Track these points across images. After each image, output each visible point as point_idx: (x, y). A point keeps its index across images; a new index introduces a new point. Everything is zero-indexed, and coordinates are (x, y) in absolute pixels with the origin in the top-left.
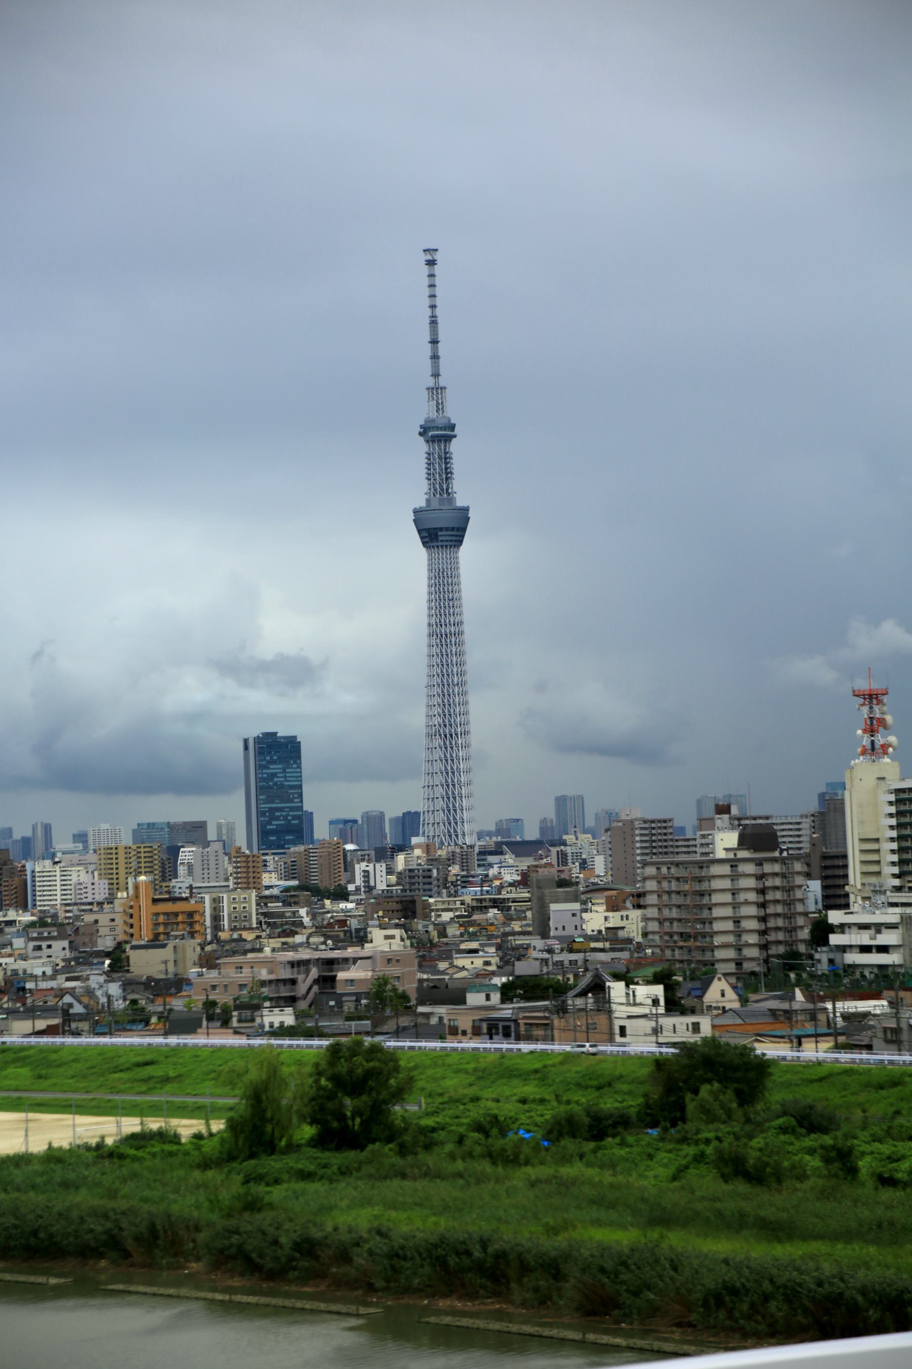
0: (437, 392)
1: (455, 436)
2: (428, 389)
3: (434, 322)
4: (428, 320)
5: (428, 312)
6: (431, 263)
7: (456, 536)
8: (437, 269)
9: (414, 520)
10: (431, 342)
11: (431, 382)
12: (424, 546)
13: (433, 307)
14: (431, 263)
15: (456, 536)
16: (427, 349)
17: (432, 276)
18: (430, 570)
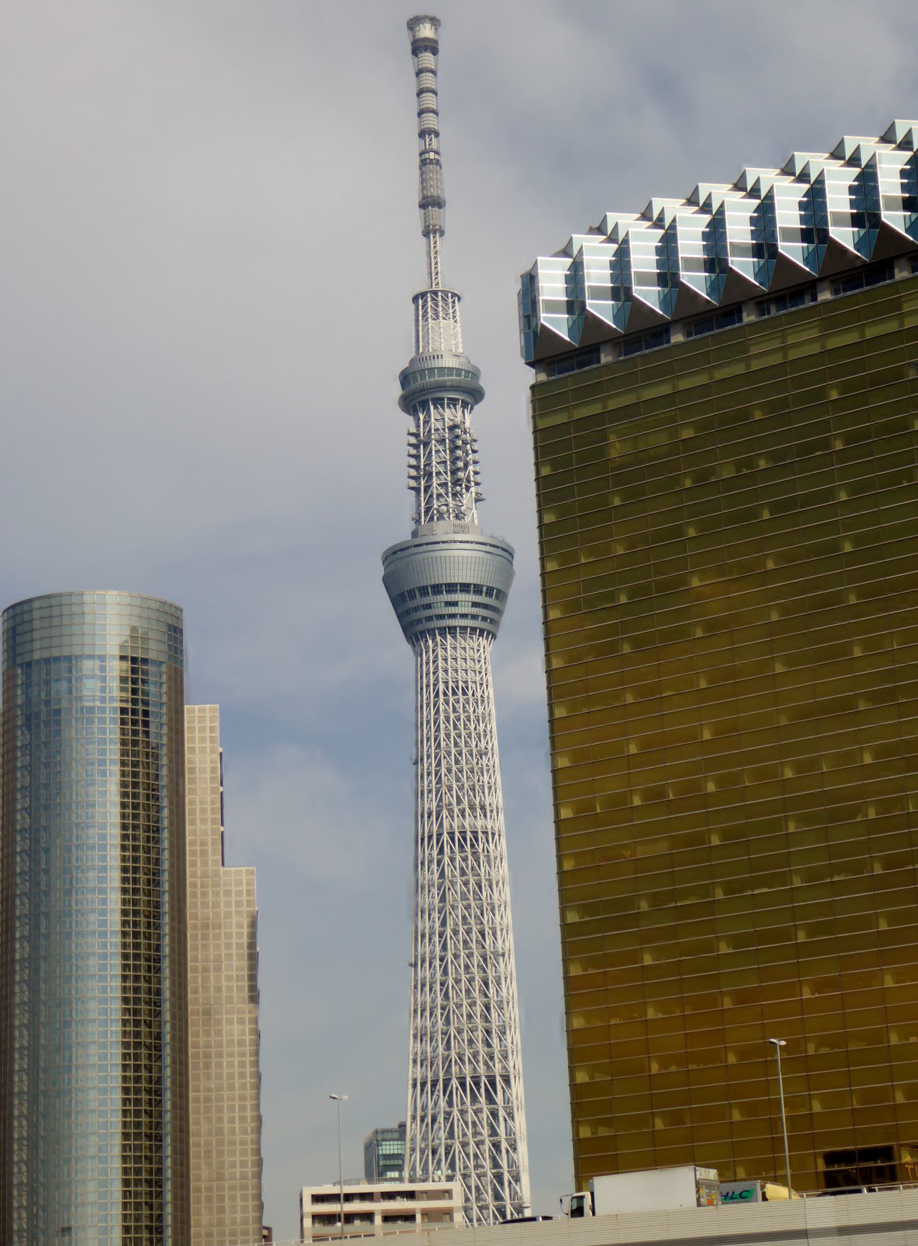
4: (417, 161)
9: (385, 580)
16: (415, 218)
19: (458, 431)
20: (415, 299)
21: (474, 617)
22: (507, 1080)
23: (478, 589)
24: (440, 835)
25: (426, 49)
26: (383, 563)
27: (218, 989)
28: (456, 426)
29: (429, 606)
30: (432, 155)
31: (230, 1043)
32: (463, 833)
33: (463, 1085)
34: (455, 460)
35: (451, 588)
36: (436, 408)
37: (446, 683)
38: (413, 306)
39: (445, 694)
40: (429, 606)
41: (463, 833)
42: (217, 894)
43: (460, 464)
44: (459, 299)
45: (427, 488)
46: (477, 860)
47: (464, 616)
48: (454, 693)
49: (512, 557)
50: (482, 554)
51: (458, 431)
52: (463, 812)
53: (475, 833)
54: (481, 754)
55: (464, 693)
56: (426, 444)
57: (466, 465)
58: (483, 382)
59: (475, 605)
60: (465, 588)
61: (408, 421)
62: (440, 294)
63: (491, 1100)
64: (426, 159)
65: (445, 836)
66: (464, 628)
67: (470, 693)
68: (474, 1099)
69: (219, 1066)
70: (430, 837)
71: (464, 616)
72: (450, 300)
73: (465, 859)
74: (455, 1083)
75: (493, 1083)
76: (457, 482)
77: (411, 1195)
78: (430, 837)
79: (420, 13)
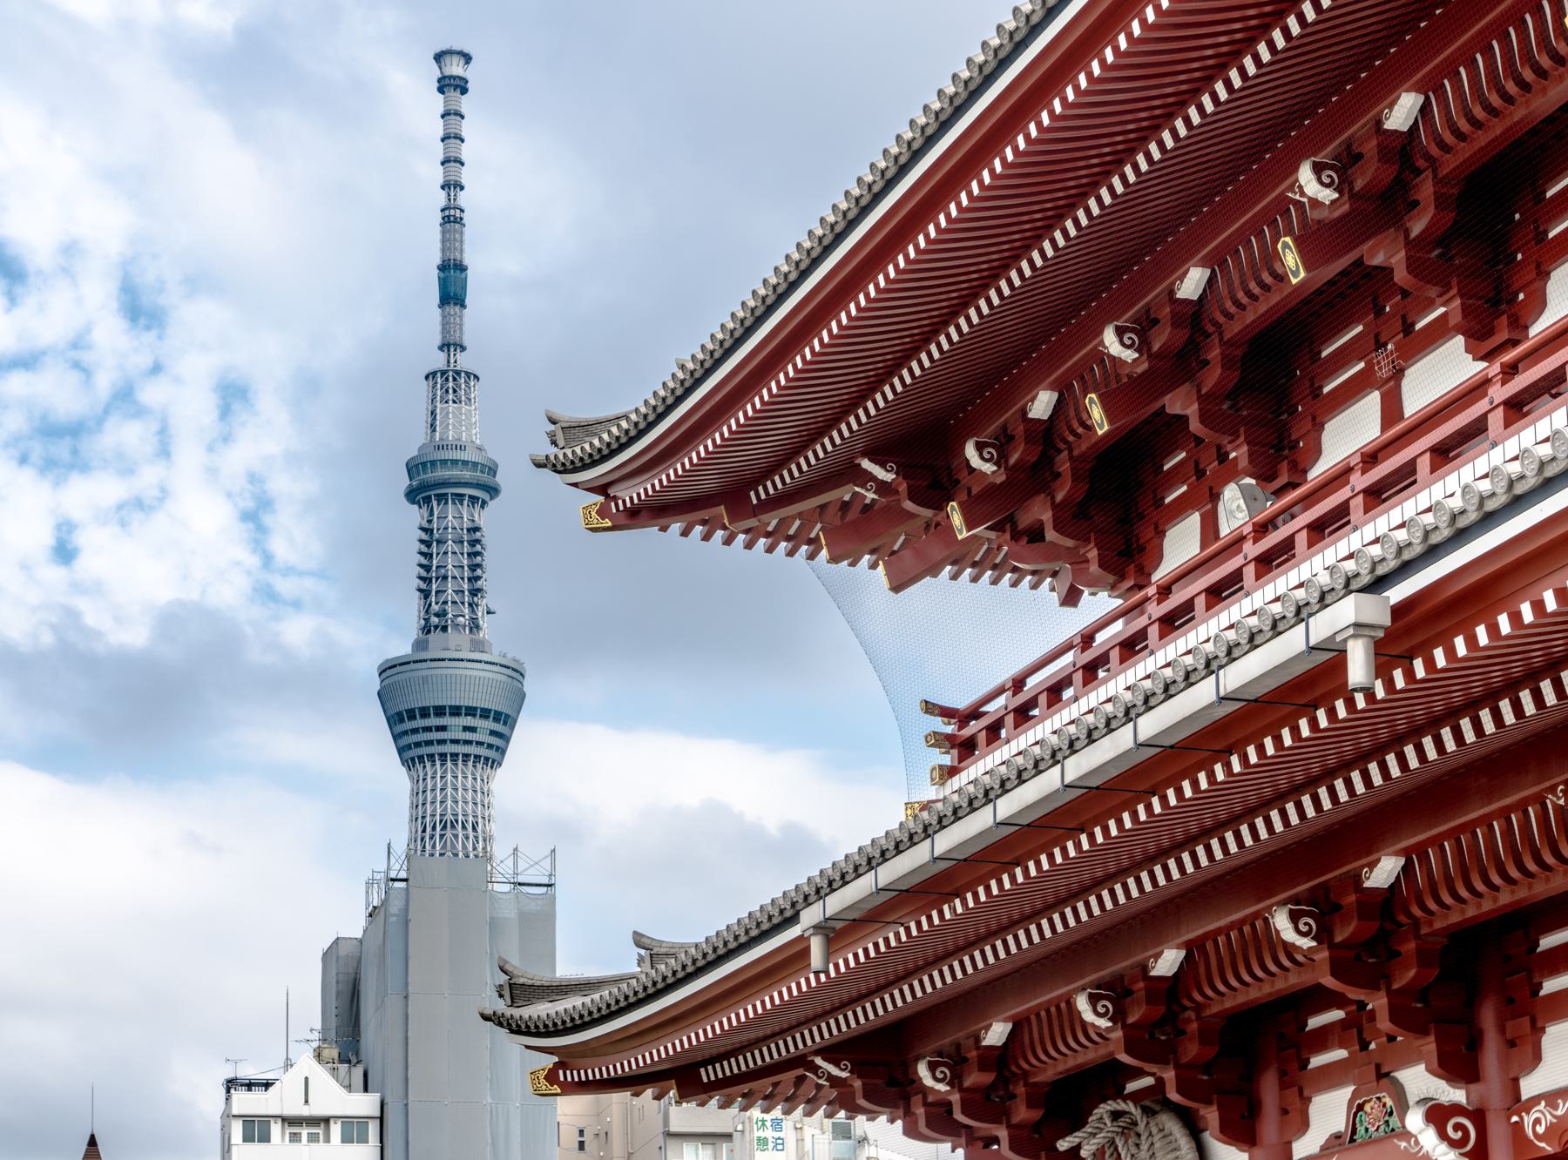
1: (493, 491)
3: (452, 219)
5: (441, 198)
6: (451, 85)
11: (438, 361)
12: (404, 762)
20: (427, 377)
21: (490, 746)
23: (498, 717)
25: (456, 87)
26: (380, 675)
29: (443, 728)
34: (473, 568)
35: (471, 711)
40: (443, 728)
47: (479, 743)
48: (464, 827)
49: (523, 676)
50: (504, 678)
59: (493, 733)
60: (485, 713)
62: (463, 375)
64: (448, 217)
66: (476, 756)
71: (479, 743)
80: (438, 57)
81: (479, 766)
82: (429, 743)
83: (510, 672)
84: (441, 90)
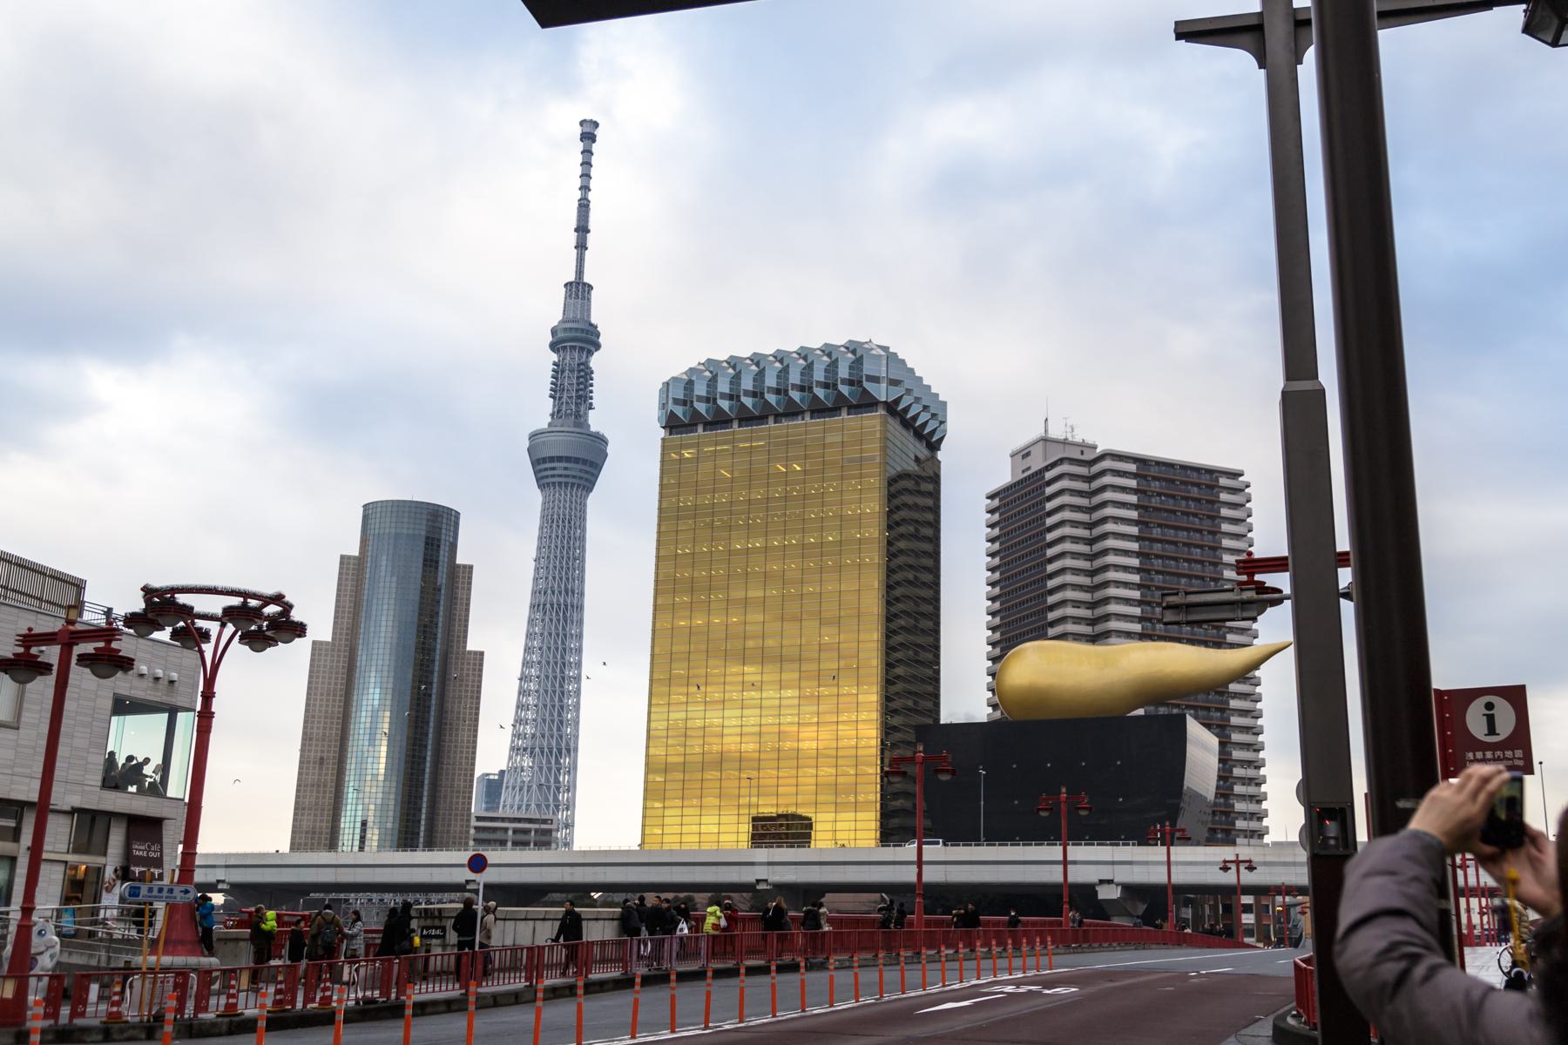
0: (579, 290)
2: (566, 285)
3: (584, 207)
4: (576, 204)
5: (578, 195)
6: (589, 134)
7: (587, 472)
8: (595, 147)
10: (576, 230)
11: (572, 278)
12: (539, 487)
13: (585, 188)
14: (589, 134)
15: (587, 472)
16: (572, 238)
17: (587, 152)
18: (543, 517)
19: (582, 367)
21: (581, 478)
22: (568, 751)
23: (585, 462)
24: (545, 605)
25: (589, 138)
26: (530, 439)
27: (459, 713)
28: (582, 364)
29: (553, 469)
30: (585, 202)
31: (462, 741)
32: (559, 605)
33: (542, 752)
34: (578, 384)
35: (568, 459)
36: (571, 351)
37: (559, 515)
38: (564, 290)
39: (558, 522)
40: (553, 469)
41: (559, 605)
42: (463, 664)
43: (582, 386)
44: (592, 288)
45: (560, 398)
46: (566, 621)
47: (574, 477)
48: (563, 522)
51: (582, 367)
52: (560, 593)
53: (566, 606)
54: (575, 559)
55: (569, 522)
56: (563, 372)
57: (586, 387)
58: (601, 340)
59: (581, 471)
61: (554, 357)
63: (557, 762)
65: (548, 606)
66: (573, 484)
67: (573, 523)
68: (549, 762)
69: (455, 752)
70: (539, 605)
72: (587, 289)
73: (559, 620)
74: (537, 749)
75: (560, 753)
76: (579, 397)
77: (530, 821)
78: (539, 605)
79: (588, 118)
80: (582, 123)
81: (580, 490)
82: (547, 477)
83: (594, 439)
84: (581, 140)
